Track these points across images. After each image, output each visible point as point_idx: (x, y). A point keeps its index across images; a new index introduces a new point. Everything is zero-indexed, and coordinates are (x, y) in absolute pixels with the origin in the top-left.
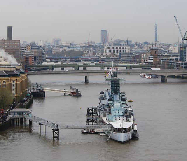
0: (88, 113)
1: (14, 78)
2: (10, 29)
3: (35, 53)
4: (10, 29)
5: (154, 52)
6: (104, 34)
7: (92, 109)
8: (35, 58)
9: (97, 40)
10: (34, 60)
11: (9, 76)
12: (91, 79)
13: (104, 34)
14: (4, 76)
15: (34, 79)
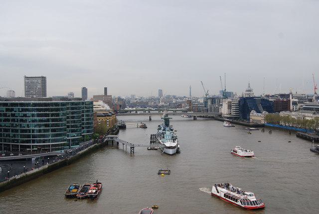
0: (151, 138)
1: (108, 117)
2: (106, 89)
3: (120, 103)
4: (106, 89)
5: (190, 102)
6: (160, 91)
7: (154, 135)
8: (120, 106)
9: (156, 95)
10: (120, 107)
11: (105, 116)
12: (153, 118)
13: (160, 92)
14: (103, 116)
15: (120, 118)
